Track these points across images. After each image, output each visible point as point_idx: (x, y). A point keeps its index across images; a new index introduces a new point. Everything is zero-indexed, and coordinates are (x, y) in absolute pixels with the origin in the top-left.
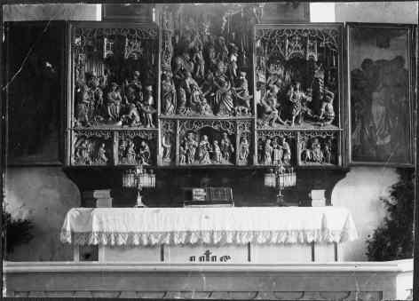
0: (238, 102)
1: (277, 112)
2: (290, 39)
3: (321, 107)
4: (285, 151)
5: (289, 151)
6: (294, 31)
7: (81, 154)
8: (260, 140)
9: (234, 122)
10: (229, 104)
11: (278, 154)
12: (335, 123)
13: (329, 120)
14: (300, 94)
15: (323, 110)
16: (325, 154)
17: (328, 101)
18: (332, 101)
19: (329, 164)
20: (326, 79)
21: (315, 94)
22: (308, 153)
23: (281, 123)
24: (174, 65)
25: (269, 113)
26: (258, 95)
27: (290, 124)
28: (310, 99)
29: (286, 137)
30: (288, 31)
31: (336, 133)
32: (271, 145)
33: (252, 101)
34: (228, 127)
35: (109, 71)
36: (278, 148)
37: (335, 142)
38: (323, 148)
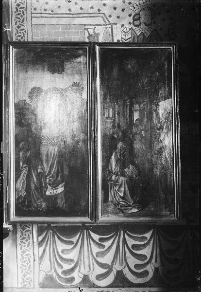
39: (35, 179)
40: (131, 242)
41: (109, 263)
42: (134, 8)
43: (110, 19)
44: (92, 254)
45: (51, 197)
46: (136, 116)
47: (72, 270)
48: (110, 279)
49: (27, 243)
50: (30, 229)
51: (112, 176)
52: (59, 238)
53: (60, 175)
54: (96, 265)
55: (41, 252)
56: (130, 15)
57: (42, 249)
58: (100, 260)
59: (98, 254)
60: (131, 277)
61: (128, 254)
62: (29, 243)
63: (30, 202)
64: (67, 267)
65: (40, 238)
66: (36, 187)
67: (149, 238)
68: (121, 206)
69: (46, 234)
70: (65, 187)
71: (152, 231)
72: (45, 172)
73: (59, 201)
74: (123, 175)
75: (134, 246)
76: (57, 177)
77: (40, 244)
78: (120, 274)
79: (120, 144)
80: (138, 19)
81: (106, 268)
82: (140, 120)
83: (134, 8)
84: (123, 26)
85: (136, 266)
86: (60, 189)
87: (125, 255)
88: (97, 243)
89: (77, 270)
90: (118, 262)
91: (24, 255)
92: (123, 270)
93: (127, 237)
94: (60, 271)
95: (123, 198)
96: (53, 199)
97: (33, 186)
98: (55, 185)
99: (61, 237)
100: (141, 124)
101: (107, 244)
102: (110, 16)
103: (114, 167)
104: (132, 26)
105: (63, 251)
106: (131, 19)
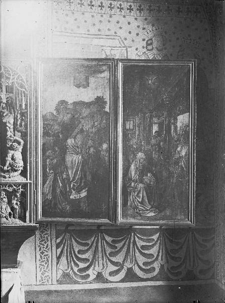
12: (24, 173)
13: (16, 171)
15: (9, 159)
16: (13, 209)
18: (20, 150)
20: (15, 124)
31: (25, 186)
37: (24, 195)
38: (10, 203)
39: (61, 185)
42: (148, 33)
43: (125, 42)
44: (106, 254)
46: (155, 128)
47: (88, 268)
48: (122, 275)
49: (46, 245)
50: (49, 232)
51: (131, 183)
52: (76, 241)
53: (83, 181)
54: (109, 263)
55: (58, 253)
56: (144, 40)
57: (59, 250)
58: (113, 259)
59: (111, 254)
62: (48, 245)
63: (55, 204)
64: (82, 265)
65: (58, 241)
66: (61, 191)
67: (156, 240)
68: (139, 211)
69: (63, 238)
70: (88, 191)
71: (158, 234)
73: (82, 204)
74: (141, 181)
76: (81, 183)
77: (58, 246)
78: (130, 270)
80: (151, 44)
81: (116, 266)
83: (148, 33)
84: (137, 49)
86: (84, 194)
87: (135, 254)
88: (110, 245)
89: (92, 268)
90: (129, 260)
91: (43, 256)
92: (133, 267)
94: (76, 269)
95: (142, 203)
97: (58, 191)
98: (79, 191)
99: (79, 240)
101: (119, 245)
102: (126, 39)
103: (133, 175)
104: (145, 50)
105: (79, 252)
106: (144, 44)
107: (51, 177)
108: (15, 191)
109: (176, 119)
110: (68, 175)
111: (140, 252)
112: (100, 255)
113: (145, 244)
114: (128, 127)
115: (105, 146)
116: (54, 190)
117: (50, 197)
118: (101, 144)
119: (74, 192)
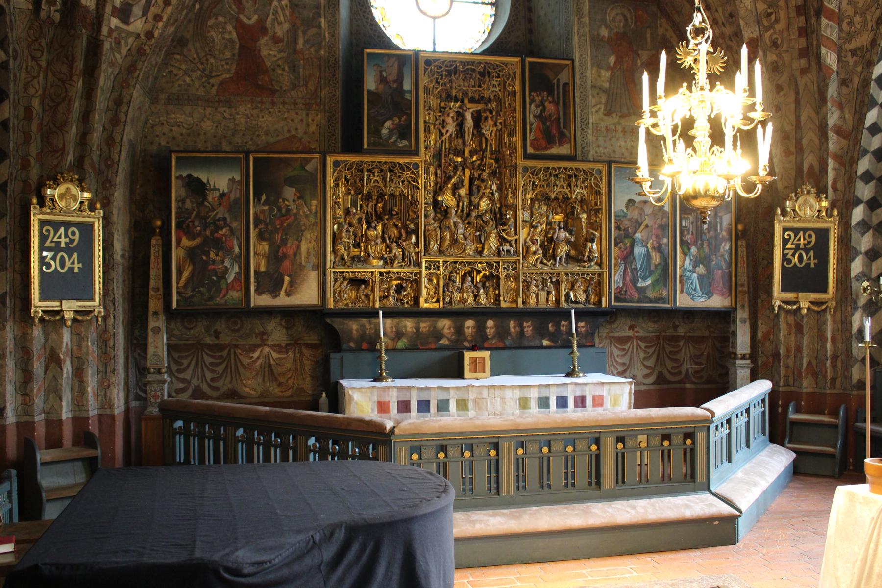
0: (502, 240)
1: (541, 252)
2: (556, 176)
3: (585, 247)
4: (549, 293)
5: (553, 292)
6: (560, 168)
7: (340, 295)
8: (525, 281)
9: (498, 263)
10: (493, 242)
11: (543, 295)
12: (600, 264)
14: (563, 234)
16: (587, 296)
17: (592, 241)
19: (591, 306)
20: (588, 218)
21: (578, 235)
22: (572, 294)
23: (546, 264)
24: (436, 204)
25: (535, 253)
26: (523, 234)
27: (554, 265)
28: (573, 239)
29: (551, 278)
30: (553, 168)
32: (536, 286)
33: (516, 241)
34: (492, 268)
35: (365, 208)
36: (543, 289)
40: (668, 349)
41: (652, 365)
45: (641, 288)
60: (668, 377)
61: (666, 358)
66: (631, 280)
72: (637, 268)
74: (694, 272)
75: (671, 352)
79: (693, 249)
82: (709, 230)
85: (673, 368)
93: (666, 345)
96: (642, 290)
97: (628, 279)
98: (645, 279)
100: (709, 232)
107: (623, 267)
108: (592, 279)
109: (721, 218)
110: (636, 265)
111: (669, 357)
112: (635, 358)
113: (673, 349)
114: (683, 225)
115: (665, 240)
116: (624, 279)
117: (621, 285)
118: (661, 239)
119: (640, 280)
